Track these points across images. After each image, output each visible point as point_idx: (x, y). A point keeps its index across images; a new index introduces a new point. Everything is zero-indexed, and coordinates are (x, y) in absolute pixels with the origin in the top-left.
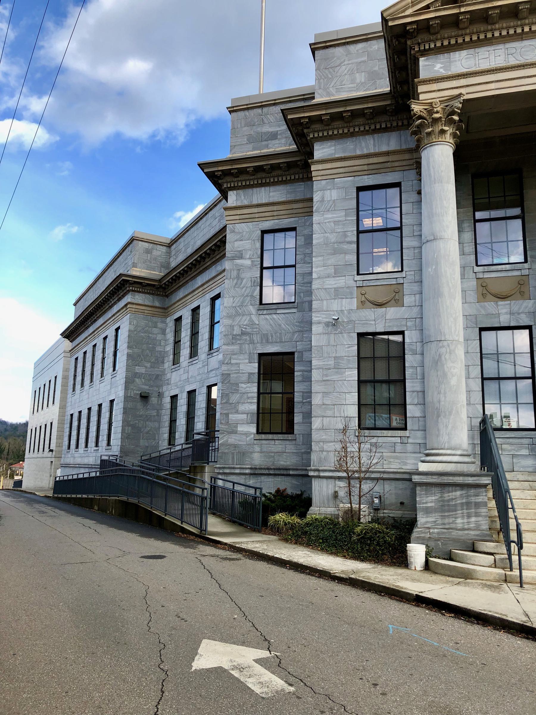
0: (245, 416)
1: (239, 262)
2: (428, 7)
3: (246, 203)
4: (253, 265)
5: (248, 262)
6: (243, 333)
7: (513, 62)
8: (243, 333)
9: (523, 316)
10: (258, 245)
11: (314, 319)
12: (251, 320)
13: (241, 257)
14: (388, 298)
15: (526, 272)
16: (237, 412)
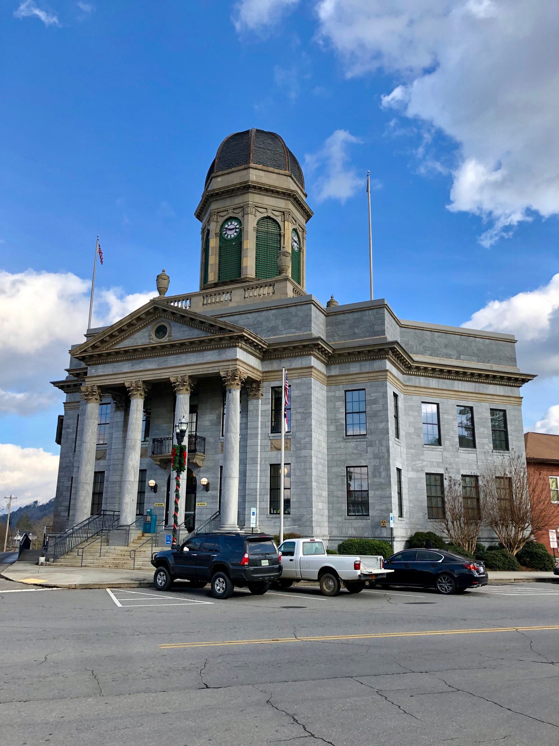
0: (64, 508)
1: (68, 430)
2: (85, 351)
3: (73, 400)
4: (73, 432)
5: (71, 430)
6: (67, 466)
7: (115, 372)
8: (67, 466)
9: (144, 465)
10: (76, 422)
11: (75, 465)
12: (70, 460)
13: (69, 428)
14: (100, 456)
15: (147, 446)
16: (61, 506)
